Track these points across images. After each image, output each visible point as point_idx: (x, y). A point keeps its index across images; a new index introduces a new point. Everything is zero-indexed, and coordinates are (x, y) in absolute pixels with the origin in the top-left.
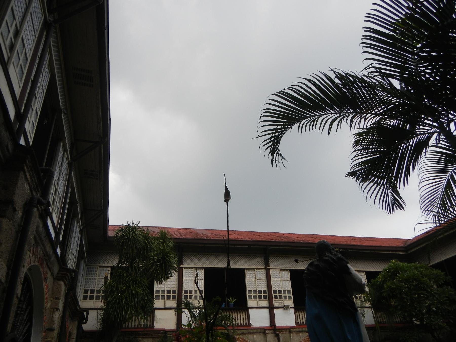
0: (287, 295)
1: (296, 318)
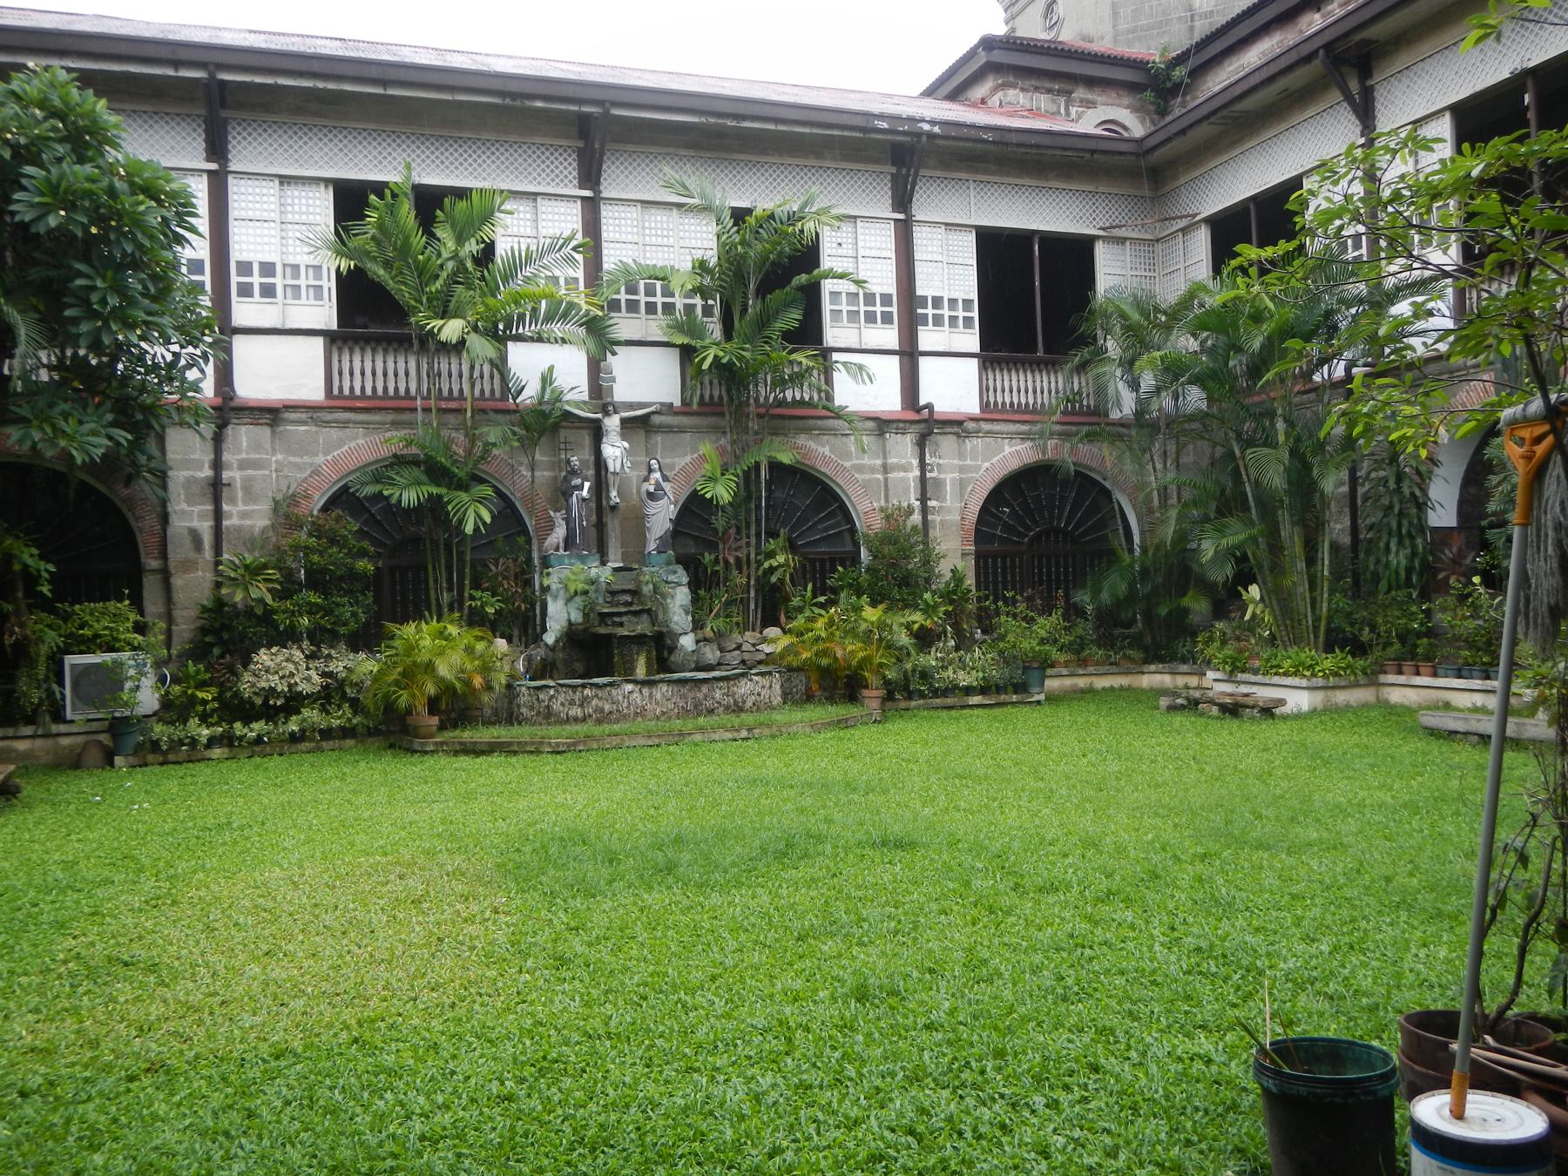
0: (961, 314)
1: (983, 390)
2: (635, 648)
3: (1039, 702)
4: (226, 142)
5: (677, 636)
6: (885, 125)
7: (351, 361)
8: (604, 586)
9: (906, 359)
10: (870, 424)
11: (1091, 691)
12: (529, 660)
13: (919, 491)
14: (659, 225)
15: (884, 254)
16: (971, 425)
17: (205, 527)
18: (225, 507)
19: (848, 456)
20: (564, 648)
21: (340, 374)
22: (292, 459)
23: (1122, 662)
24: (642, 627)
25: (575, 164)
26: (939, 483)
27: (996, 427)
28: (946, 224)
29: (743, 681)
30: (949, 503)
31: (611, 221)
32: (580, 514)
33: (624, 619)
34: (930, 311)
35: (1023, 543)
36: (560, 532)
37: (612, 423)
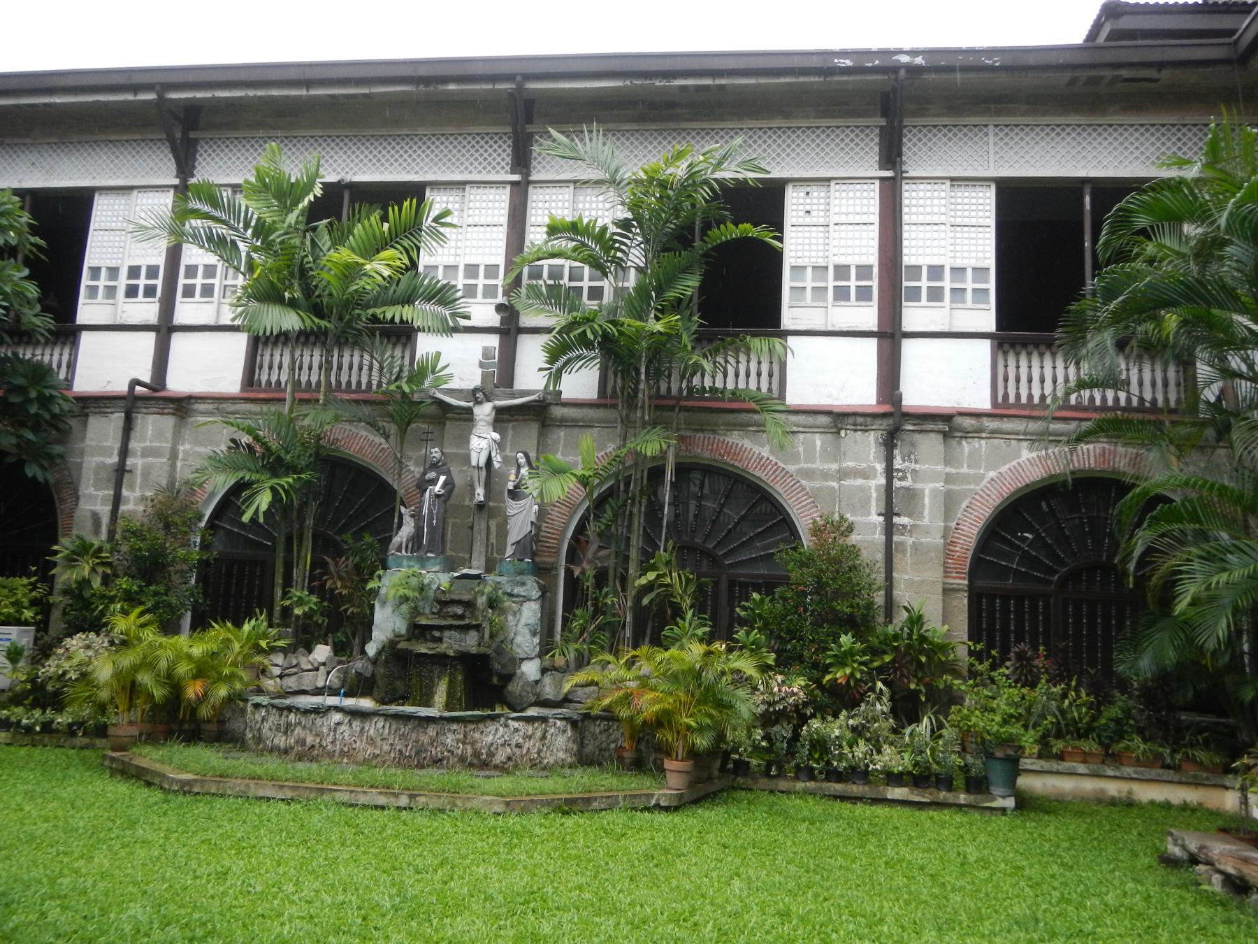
2: (437, 670)
3: (1003, 810)
4: (195, 159)
5: (517, 661)
6: (848, 63)
7: (272, 356)
8: (431, 594)
9: (887, 342)
10: (823, 420)
11: (1129, 804)
12: (346, 672)
13: (883, 504)
14: (594, 205)
15: (865, 219)
16: (968, 422)
17: (105, 510)
18: (125, 492)
19: (794, 458)
20: (387, 662)
21: (261, 368)
22: (198, 449)
23: (1185, 766)
24: (470, 642)
25: (509, 151)
26: (912, 496)
27: (1007, 425)
28: (952, 179)
29: (492, 727)
30: (926, 521)
31: (540, 205)
32: (430, 512)
33: (447, 633)
34: (924, 283)
35: (1050, 582)
36: (407, 529)
37: (484, 412)
